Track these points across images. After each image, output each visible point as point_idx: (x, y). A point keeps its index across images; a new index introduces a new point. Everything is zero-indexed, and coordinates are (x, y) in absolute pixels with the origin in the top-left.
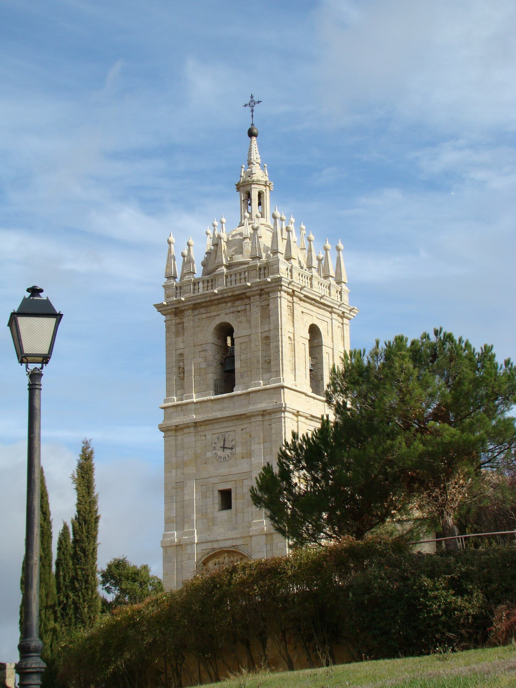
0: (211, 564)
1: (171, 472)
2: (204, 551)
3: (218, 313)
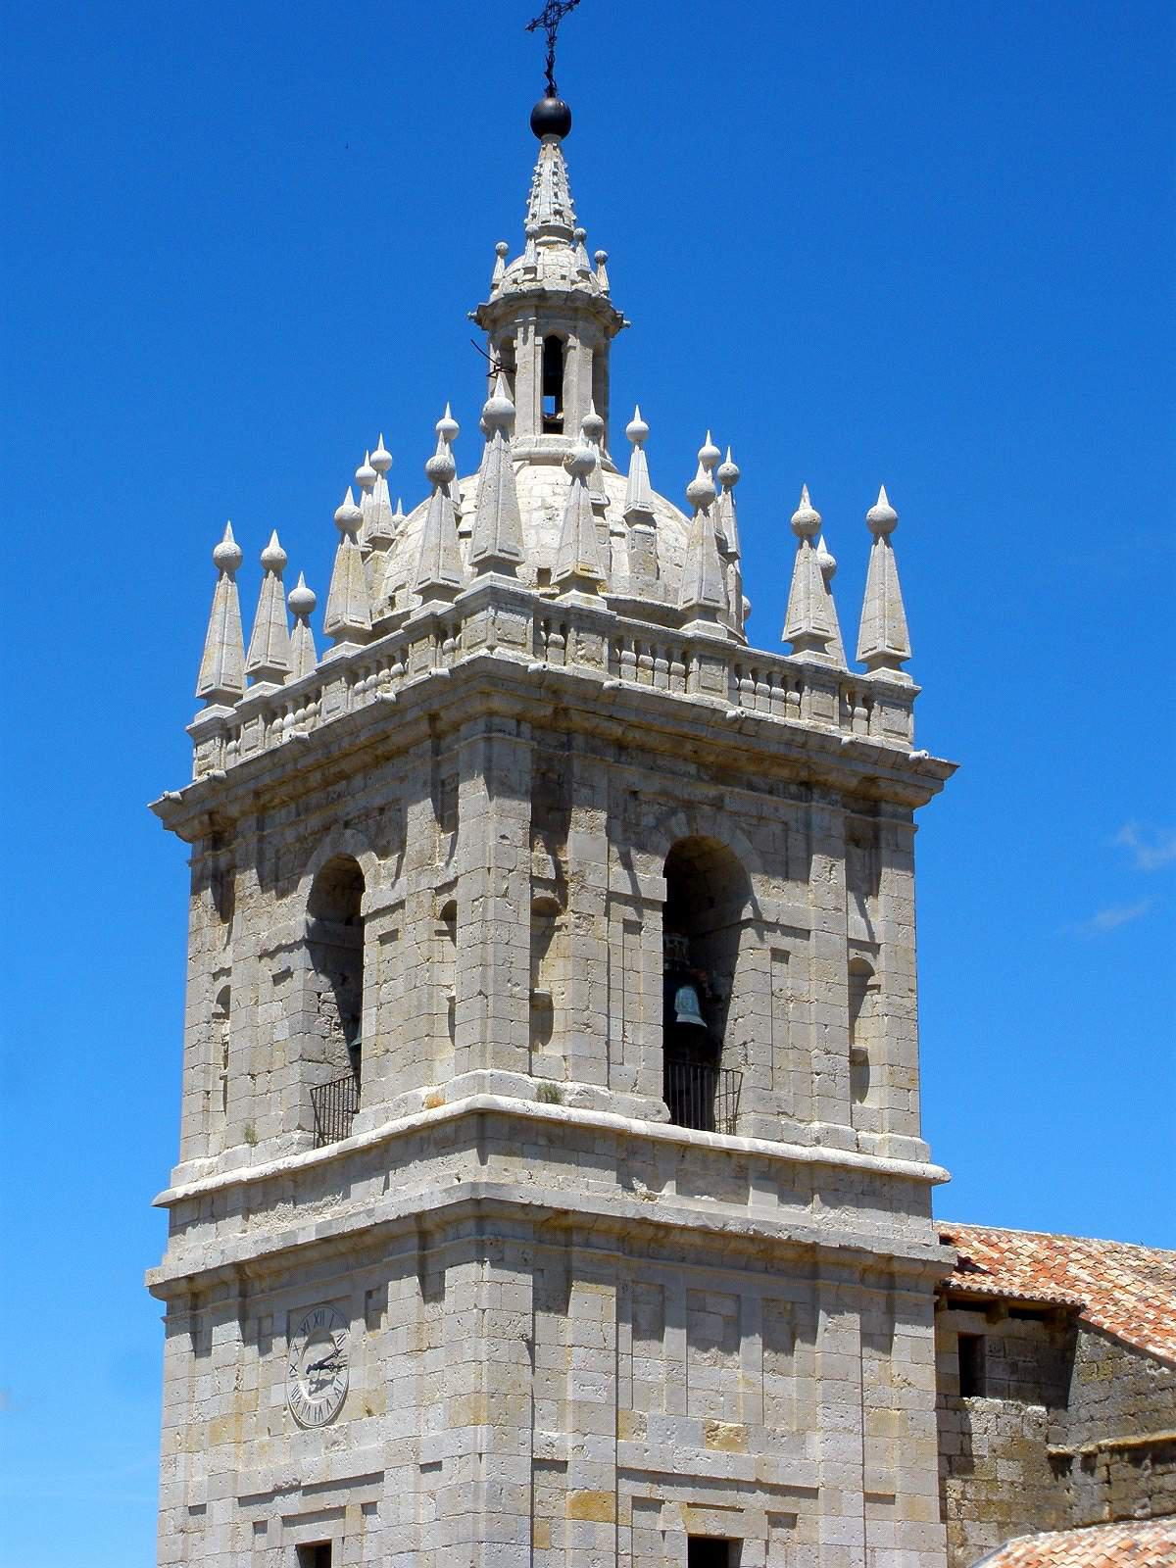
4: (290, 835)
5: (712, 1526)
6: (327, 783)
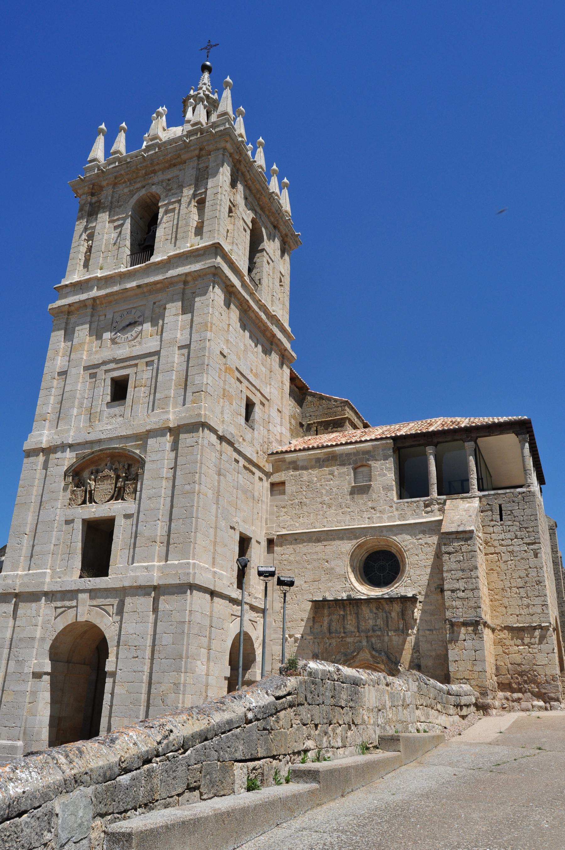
4: (126, 190)
5: (252, 397)
6: (146, 174)
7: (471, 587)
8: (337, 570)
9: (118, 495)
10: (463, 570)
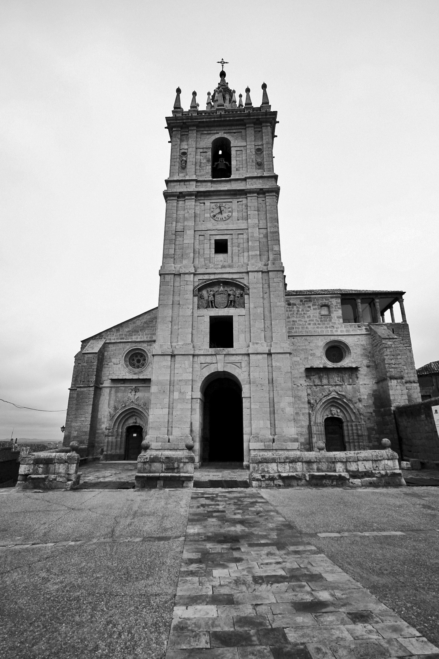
0: (204, 292)
1: (172, 224)
2: (200, 281)
3: (218, 132)
7: (398, 363)
8: (317, 354)
9: (231, 304)
10: (393, 356)
